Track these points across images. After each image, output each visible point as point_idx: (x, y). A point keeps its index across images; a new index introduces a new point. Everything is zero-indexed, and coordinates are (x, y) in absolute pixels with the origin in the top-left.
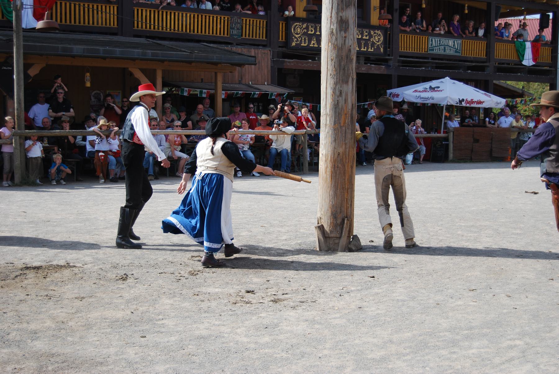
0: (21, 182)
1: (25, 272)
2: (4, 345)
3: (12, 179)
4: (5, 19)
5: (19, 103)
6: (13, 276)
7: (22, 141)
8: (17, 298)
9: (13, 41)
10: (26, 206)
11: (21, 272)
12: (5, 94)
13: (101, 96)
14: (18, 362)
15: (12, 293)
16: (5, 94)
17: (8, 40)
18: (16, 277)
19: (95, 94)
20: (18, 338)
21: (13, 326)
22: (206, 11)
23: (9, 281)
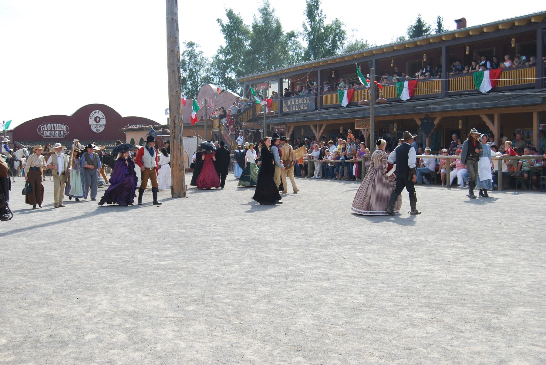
4: (475, 89)
13: (521, 132)
19: (518, 131)
22: (510, 68)
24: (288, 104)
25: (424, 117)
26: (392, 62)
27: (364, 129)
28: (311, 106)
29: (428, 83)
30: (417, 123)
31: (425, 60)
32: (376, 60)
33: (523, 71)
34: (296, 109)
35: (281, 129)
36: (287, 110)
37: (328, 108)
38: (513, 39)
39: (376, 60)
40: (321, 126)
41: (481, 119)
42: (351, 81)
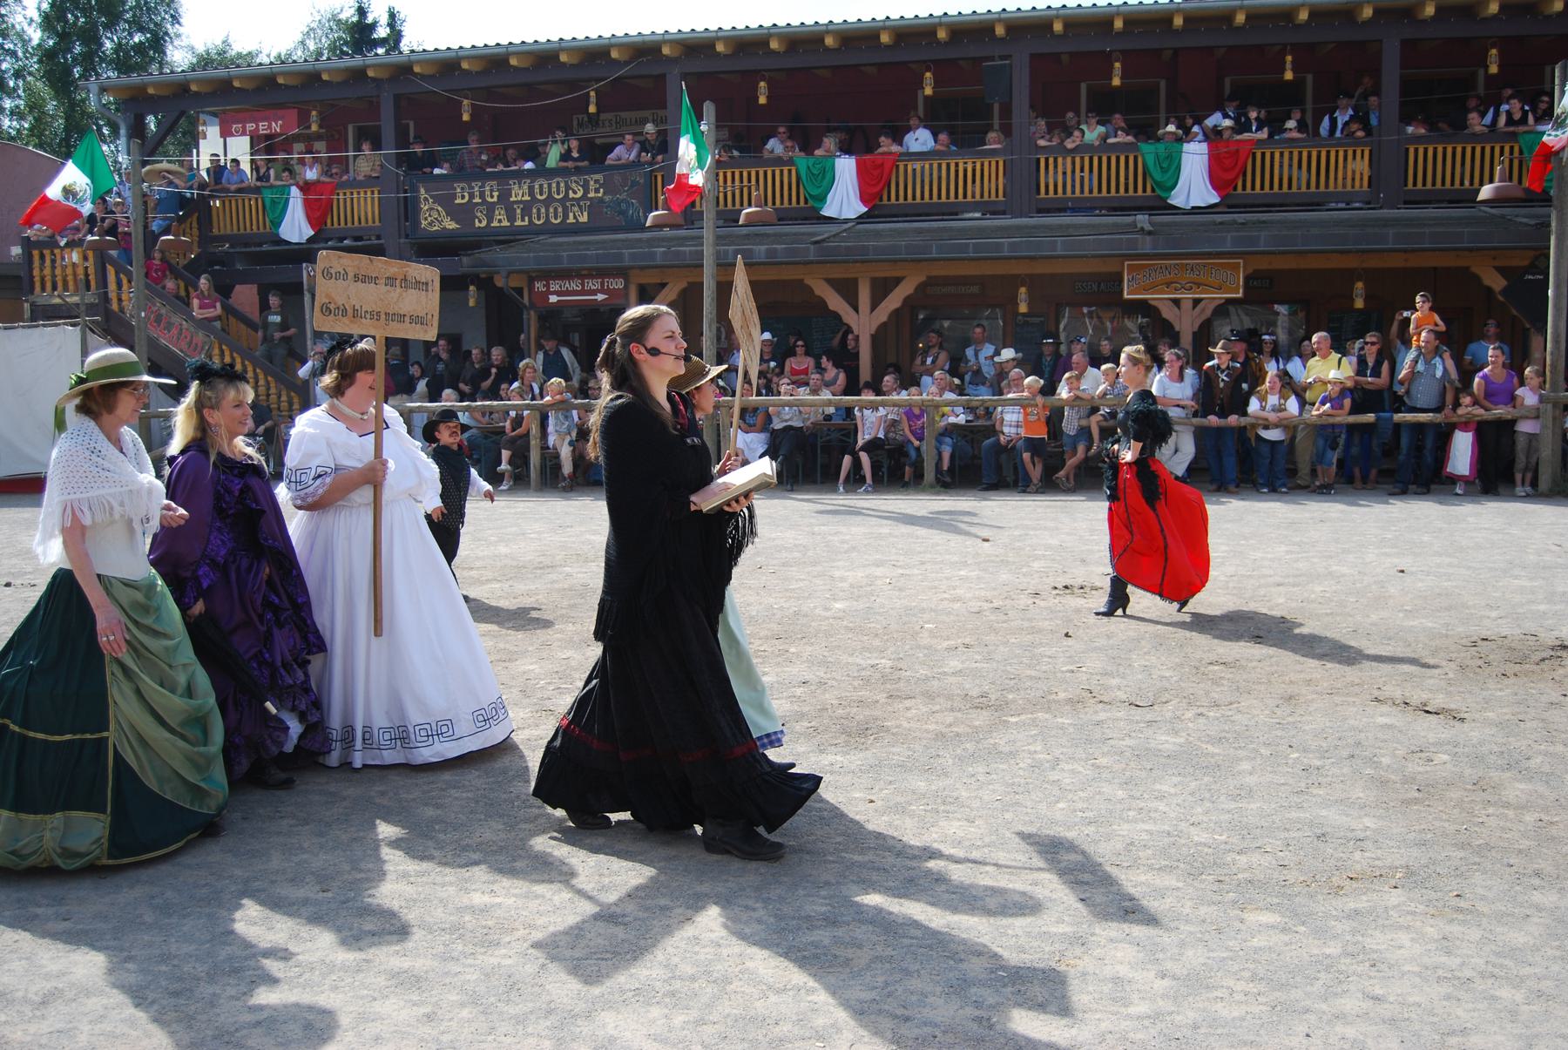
0: (1551, 490)
1: (1559, 654)
2: (1520, 777)
3: (1534, 484)
5: (1556, 341)
6: (1537, 656)
7: (1558, 413)
8: (1544, 699)
9: (1549, 225)
10: (1562, 535)
11: (1552, 653)
12: (1528, 326)
14: (1546, 810)
15: (1534, 688)
16: (1528, 326)
17: (1537, 224)
18: (1543, 660)
20: (1546, 768)
21: (1536, 746)
23: (1528, 666)
24: (458, 201)
25: (1526, 263)
26: (1288, 66)
27: (1176, 302)
28: (623, 213)
29: (944, 167)
30: (1487, 282)
31: (928, 91)
32: (1033, 56)
33: (986, 164)
34: (511, 218)
35: (594, 292)
36: (506, 223)
37: (1245, 206)
38: (928, 75)
39: (1033, 56)
40: (882, 289)
41: (811, 291)
42: (598, 141)
